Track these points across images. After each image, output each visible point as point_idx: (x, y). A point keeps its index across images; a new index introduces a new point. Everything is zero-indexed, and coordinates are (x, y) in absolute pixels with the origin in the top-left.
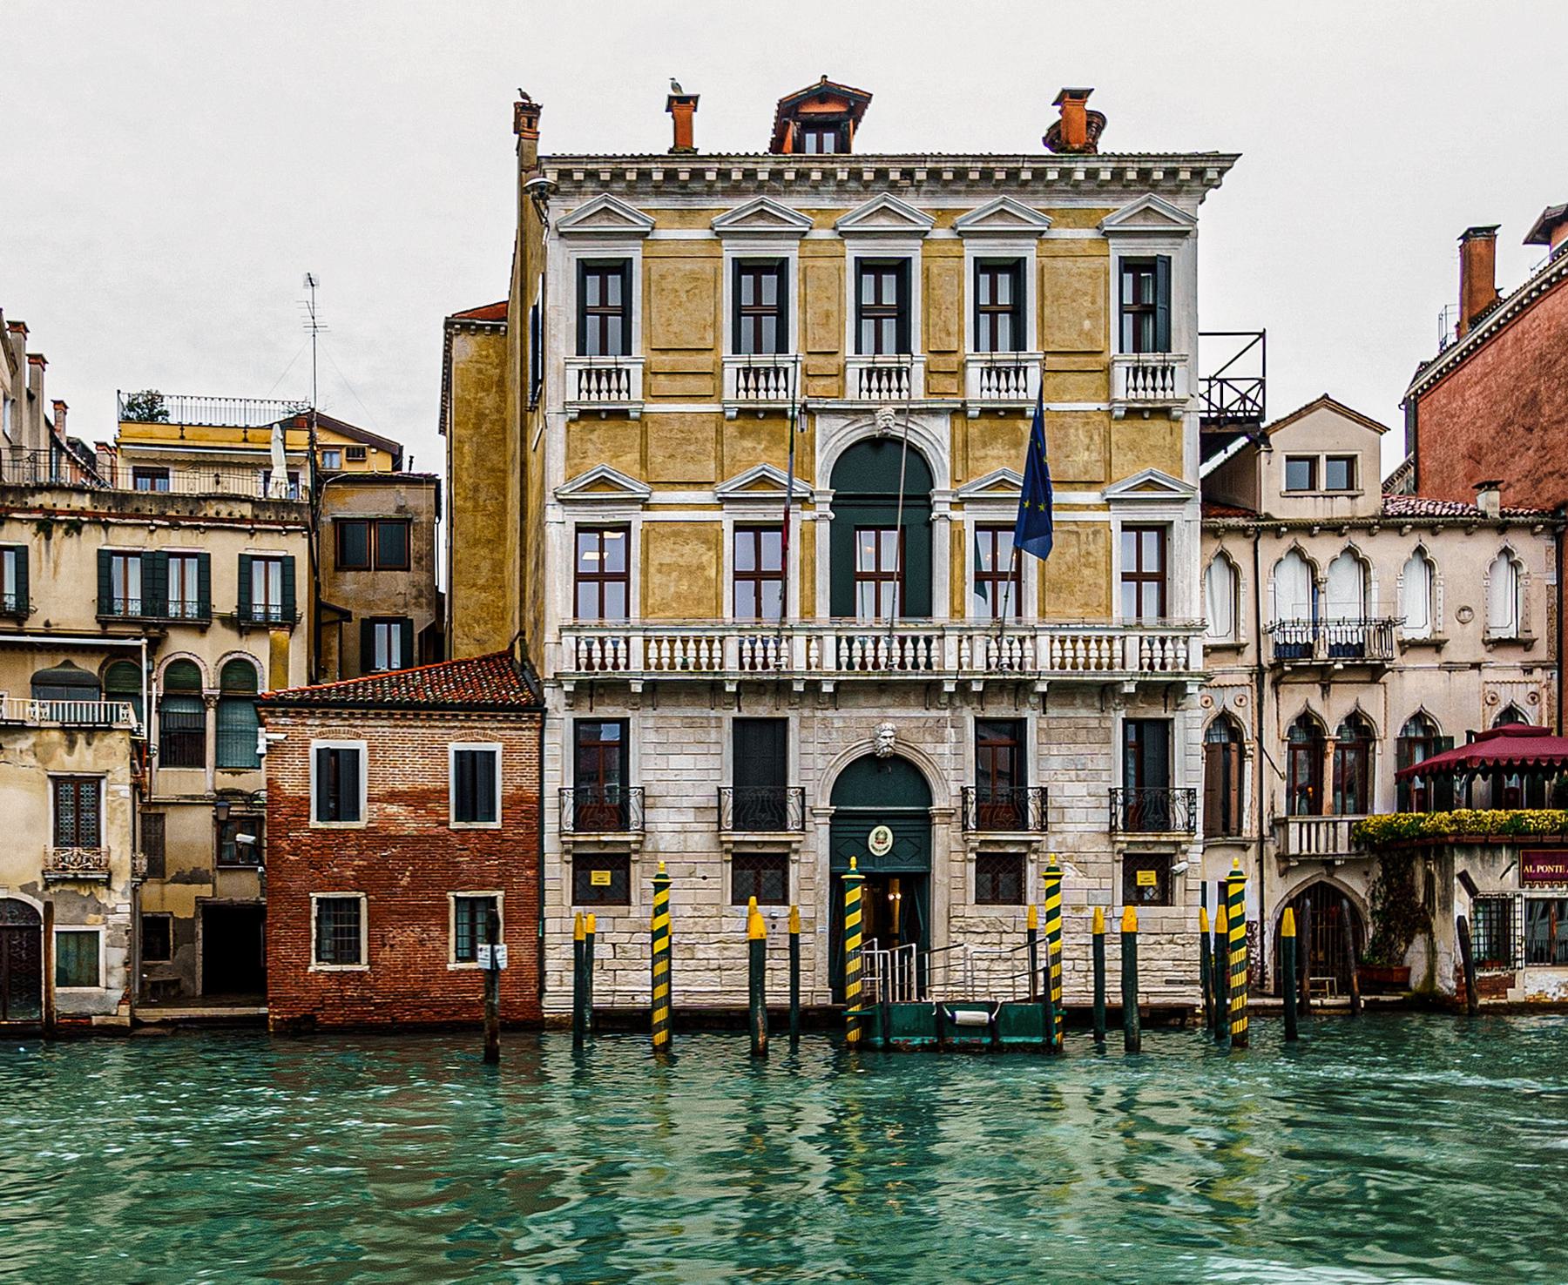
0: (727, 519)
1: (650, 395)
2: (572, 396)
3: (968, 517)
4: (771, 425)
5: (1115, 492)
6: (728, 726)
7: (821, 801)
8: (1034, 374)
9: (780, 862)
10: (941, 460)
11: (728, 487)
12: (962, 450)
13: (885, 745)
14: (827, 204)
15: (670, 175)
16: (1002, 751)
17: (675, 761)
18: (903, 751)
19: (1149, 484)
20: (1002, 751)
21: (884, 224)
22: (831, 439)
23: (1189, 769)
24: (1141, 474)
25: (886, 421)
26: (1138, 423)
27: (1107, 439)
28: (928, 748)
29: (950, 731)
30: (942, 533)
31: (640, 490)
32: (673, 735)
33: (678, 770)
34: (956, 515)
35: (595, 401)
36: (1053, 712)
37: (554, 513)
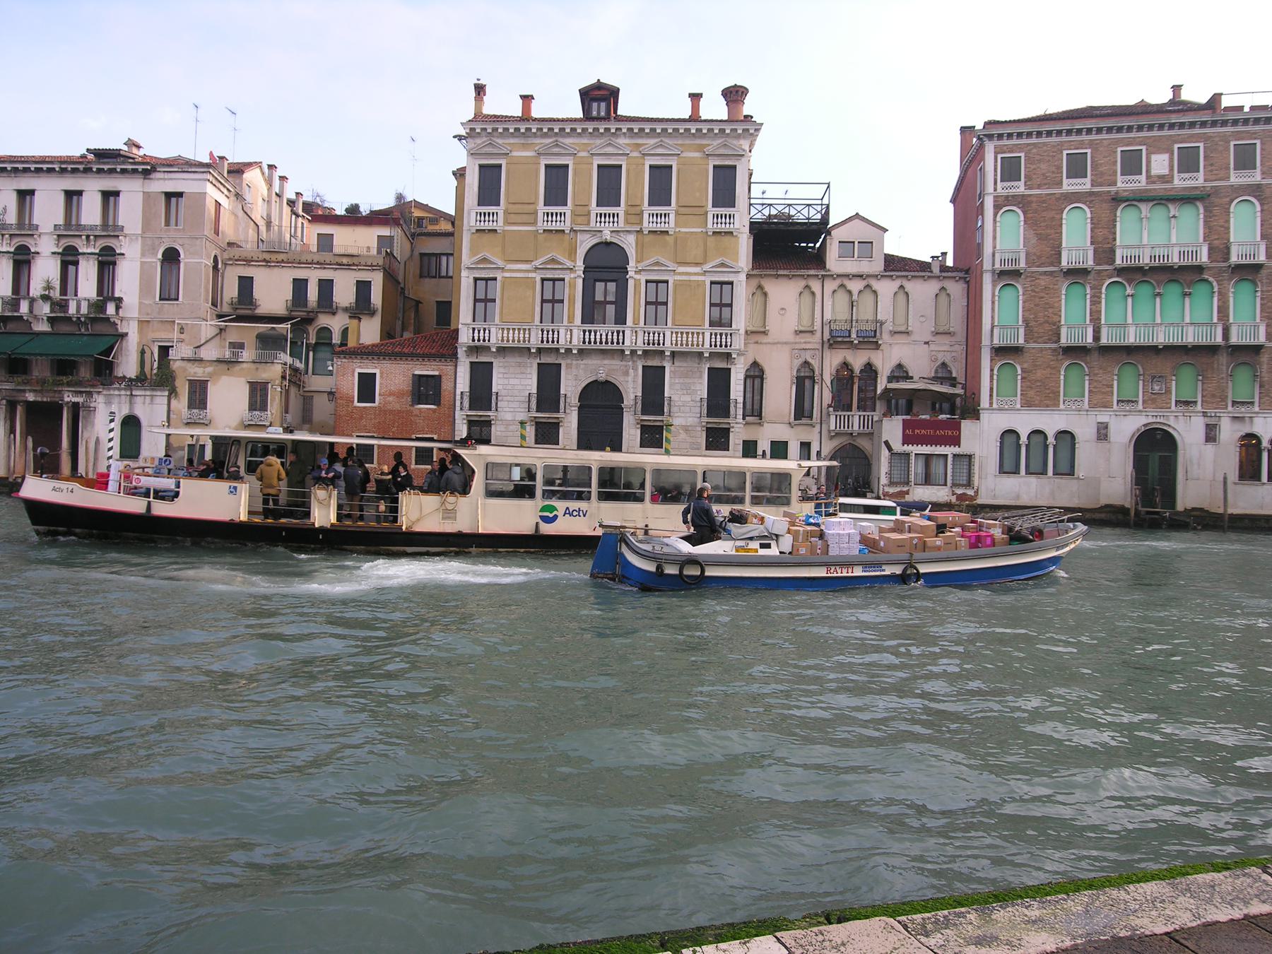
0: (538, 277)
1: (507, 222)
2: (473, 223)
3: (642, 278)
4: (560, 235)
5: (707, 267)
6: (535, 367)
7: (574, 400)
8: (672, 216)
9: (556, 426)
10: (631, 253)
11: (537, 263)
12: (640, 246)
13: (602, 376)
14: (585, 141)
15: (517, 130)
16: (653, 381)
17: (512, 381)
18: (610, 379)
19: (723, 265)
20: (653, 381)
21: (610, 150)
22: (585, 243)
23: (737, 390)
24: (718, 261)
25: (607, 236)
26: (718, 237)
27: (705, 245)
28: (621, 379)
29: (631, 371)
30: (631, 283)
31: (501, 263)
32: (512, 370)
33: (515, 386)
34: (637, 277)
35: (483, 226)
36: (677, 364)
37: (464, 273)
